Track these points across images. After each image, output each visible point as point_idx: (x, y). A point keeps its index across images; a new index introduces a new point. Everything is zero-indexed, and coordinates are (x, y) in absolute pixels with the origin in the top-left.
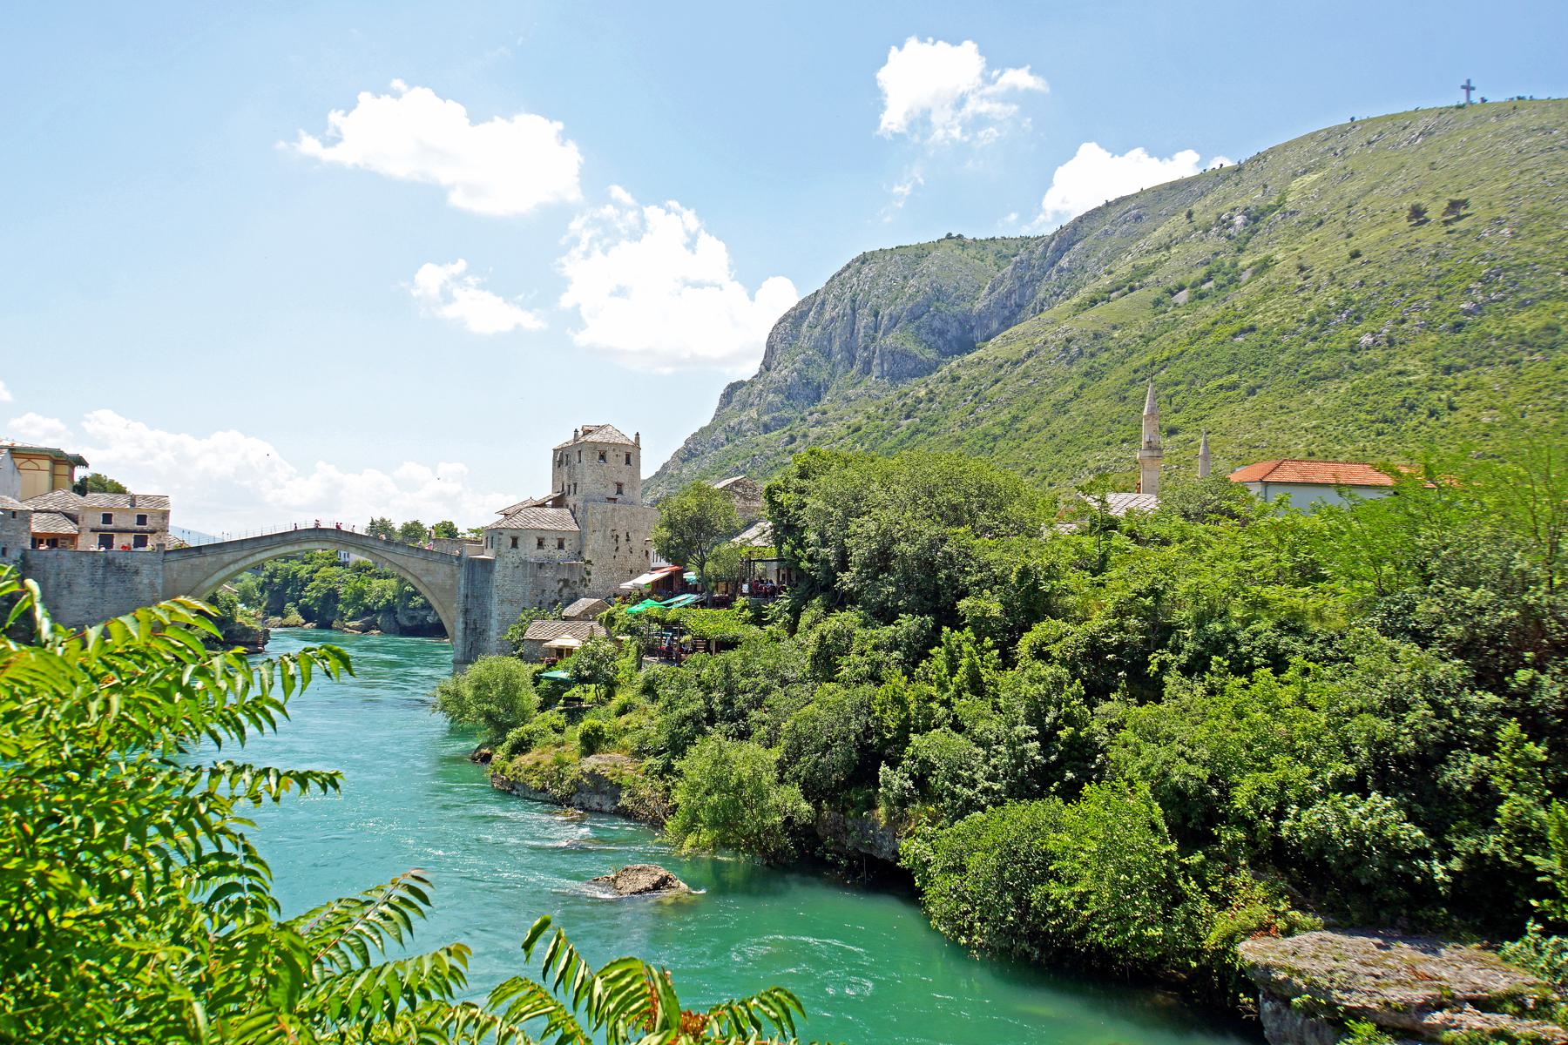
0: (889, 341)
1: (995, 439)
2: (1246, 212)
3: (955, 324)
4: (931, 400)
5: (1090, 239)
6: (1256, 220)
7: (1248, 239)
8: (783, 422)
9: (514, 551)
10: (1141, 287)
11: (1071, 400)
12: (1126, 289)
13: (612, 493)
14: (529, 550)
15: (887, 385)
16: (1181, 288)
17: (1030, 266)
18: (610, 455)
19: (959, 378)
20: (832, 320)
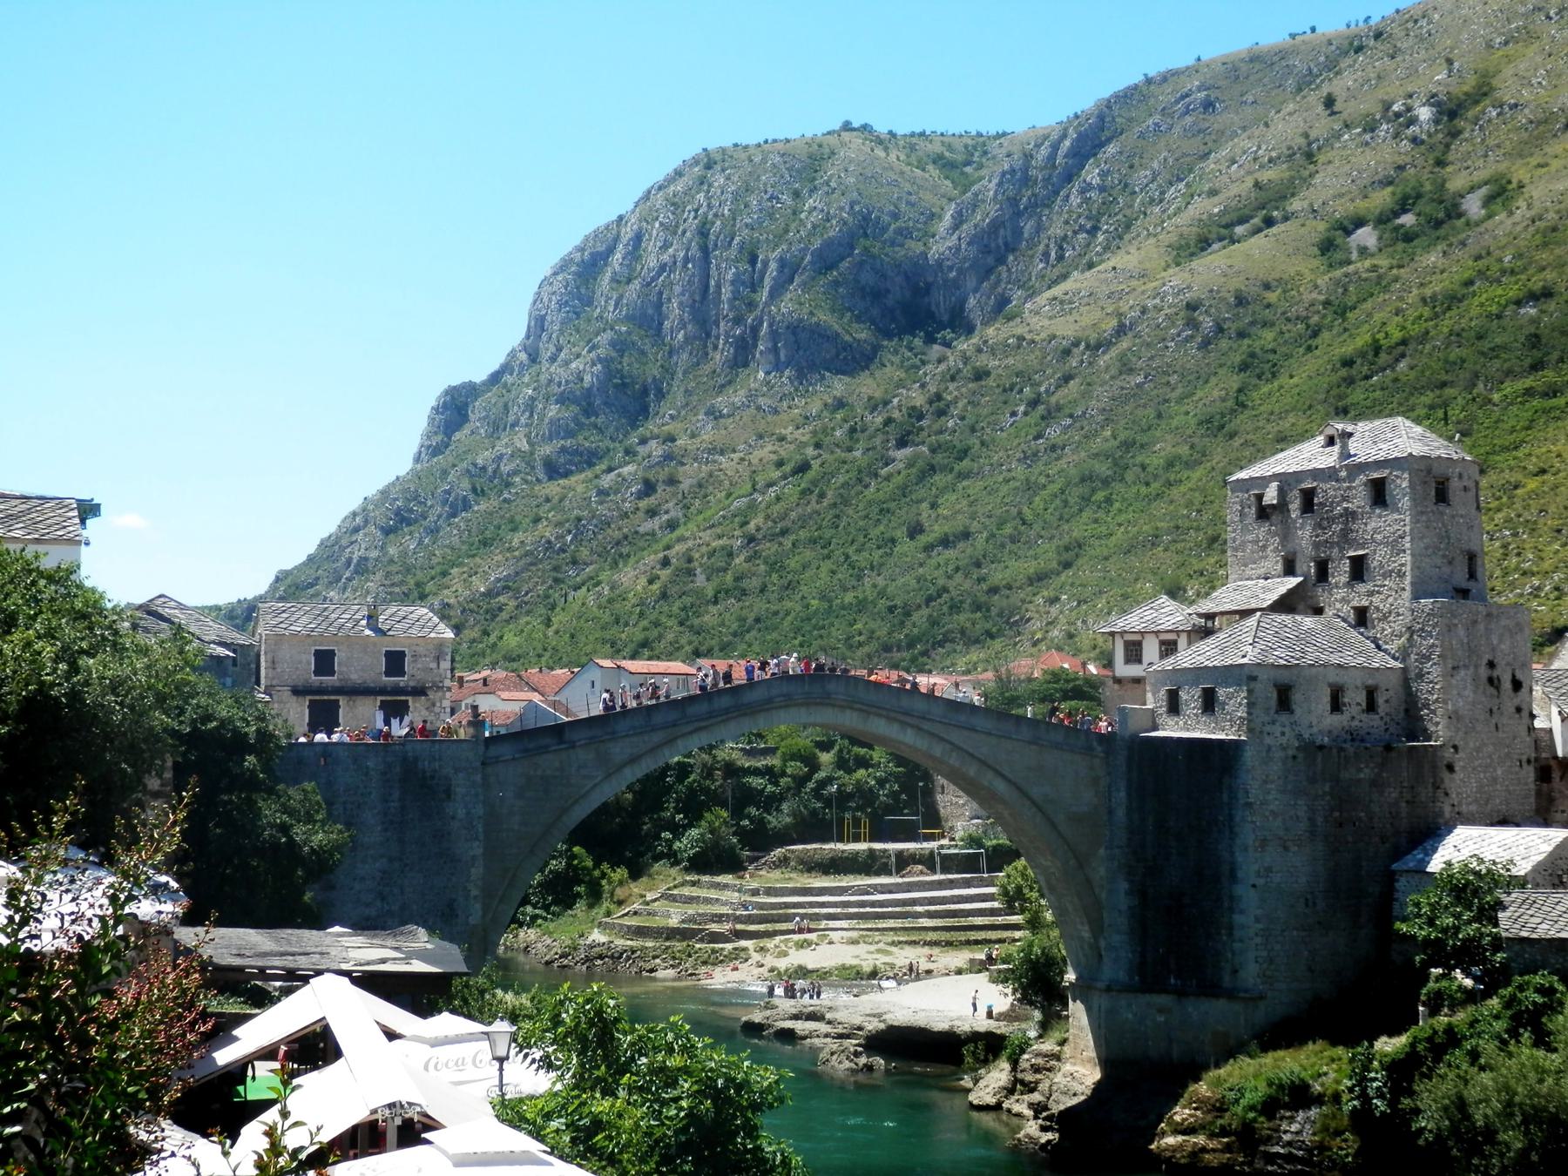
0: (787, 306)
1: (1106, 482)
2: (1432, 100)
3: (899, 279)
4: (941, 413)
5: (1129, 138)
6: (1453, 115)
7: (1447, 146)
8: (590, 459)
9: (1284, 718)
10: (1286, 219)
11: (1233, 411)
12: (1256, 221)
13: (1460, 578)
14: (1315, 716)
15: (789, 389)
16: (1359, 223)
17: (1026, 180)
18: (1455, 485)
19: (988, 374)
20: (663, 268)
